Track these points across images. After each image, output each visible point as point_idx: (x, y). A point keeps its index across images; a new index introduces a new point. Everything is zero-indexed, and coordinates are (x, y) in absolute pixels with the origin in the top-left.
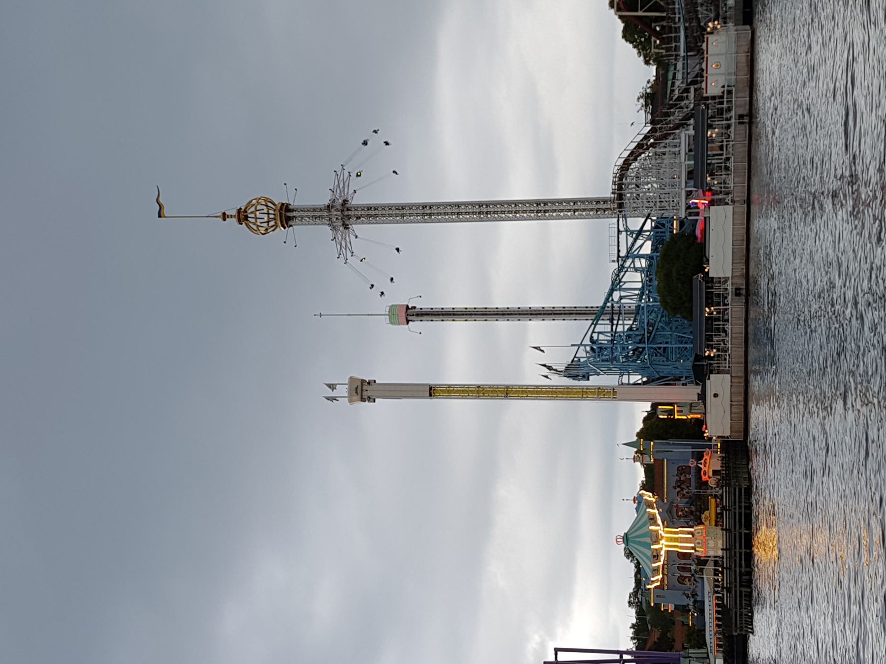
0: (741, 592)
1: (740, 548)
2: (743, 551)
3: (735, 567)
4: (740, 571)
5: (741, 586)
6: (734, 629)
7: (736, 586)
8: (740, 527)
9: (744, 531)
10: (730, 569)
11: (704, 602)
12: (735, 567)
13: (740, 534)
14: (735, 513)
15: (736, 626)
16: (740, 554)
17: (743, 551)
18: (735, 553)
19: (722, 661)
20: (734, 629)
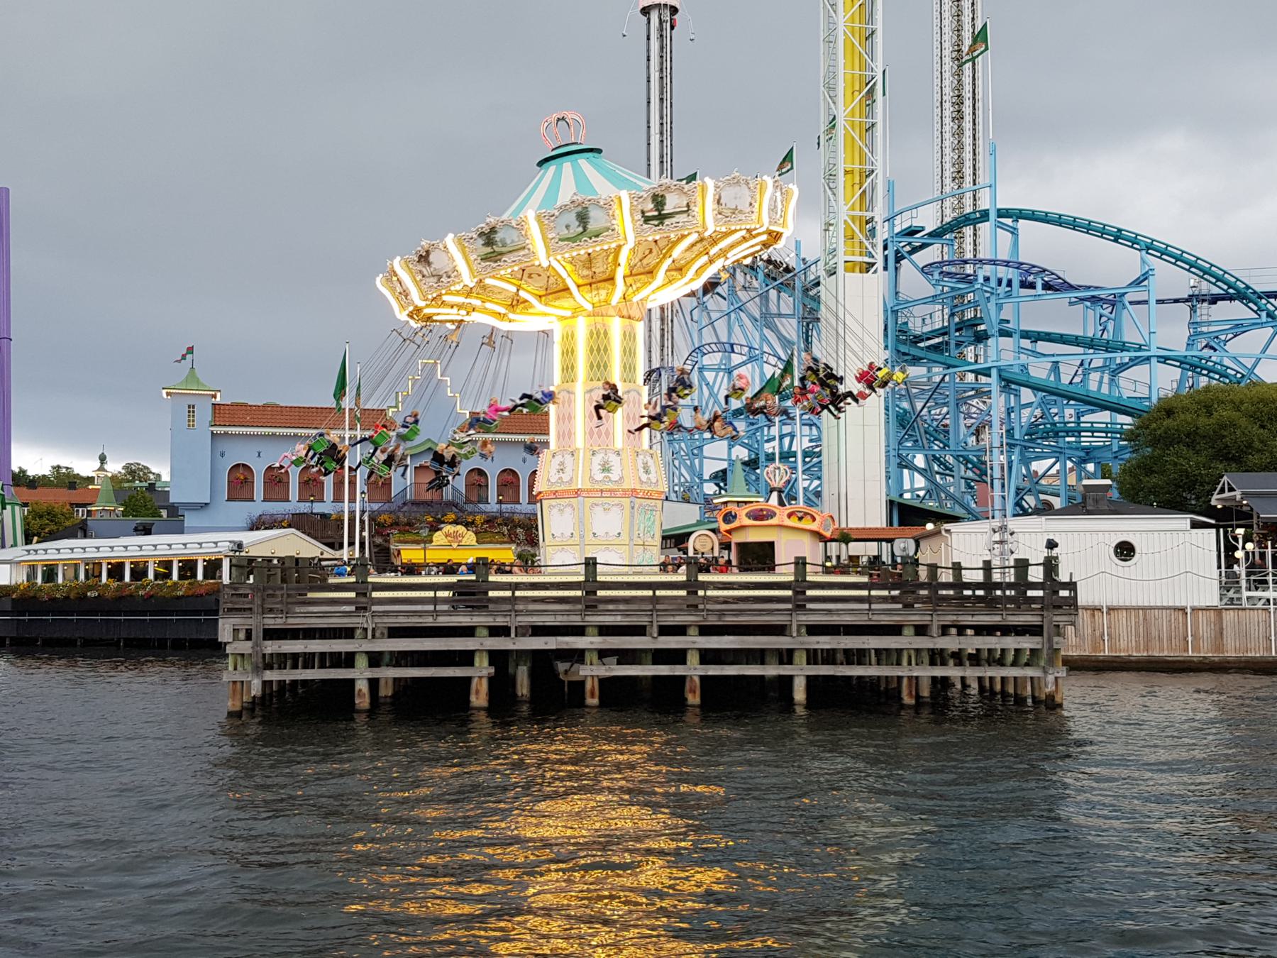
0: (466, 658)
1: (708, 657)
2: (693, 670)
3: (605, 631)
4: (577, 656)
5: (497, 657)
6: (253, 622)
7: (496, 631)
8: (813, 657)
9: (800, 672)
10: (591, 604)
11: (182, 533)
12: (605, 631)
13: (786, 657)
14: (895, 630)
15: (271, 634)
16: (678, 657)
17: (693, 670)
18: (680, 630)
19: (5, 582)
20: (253, 622)
